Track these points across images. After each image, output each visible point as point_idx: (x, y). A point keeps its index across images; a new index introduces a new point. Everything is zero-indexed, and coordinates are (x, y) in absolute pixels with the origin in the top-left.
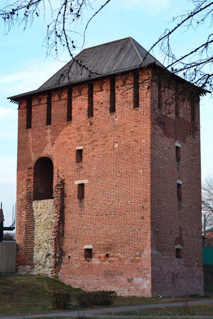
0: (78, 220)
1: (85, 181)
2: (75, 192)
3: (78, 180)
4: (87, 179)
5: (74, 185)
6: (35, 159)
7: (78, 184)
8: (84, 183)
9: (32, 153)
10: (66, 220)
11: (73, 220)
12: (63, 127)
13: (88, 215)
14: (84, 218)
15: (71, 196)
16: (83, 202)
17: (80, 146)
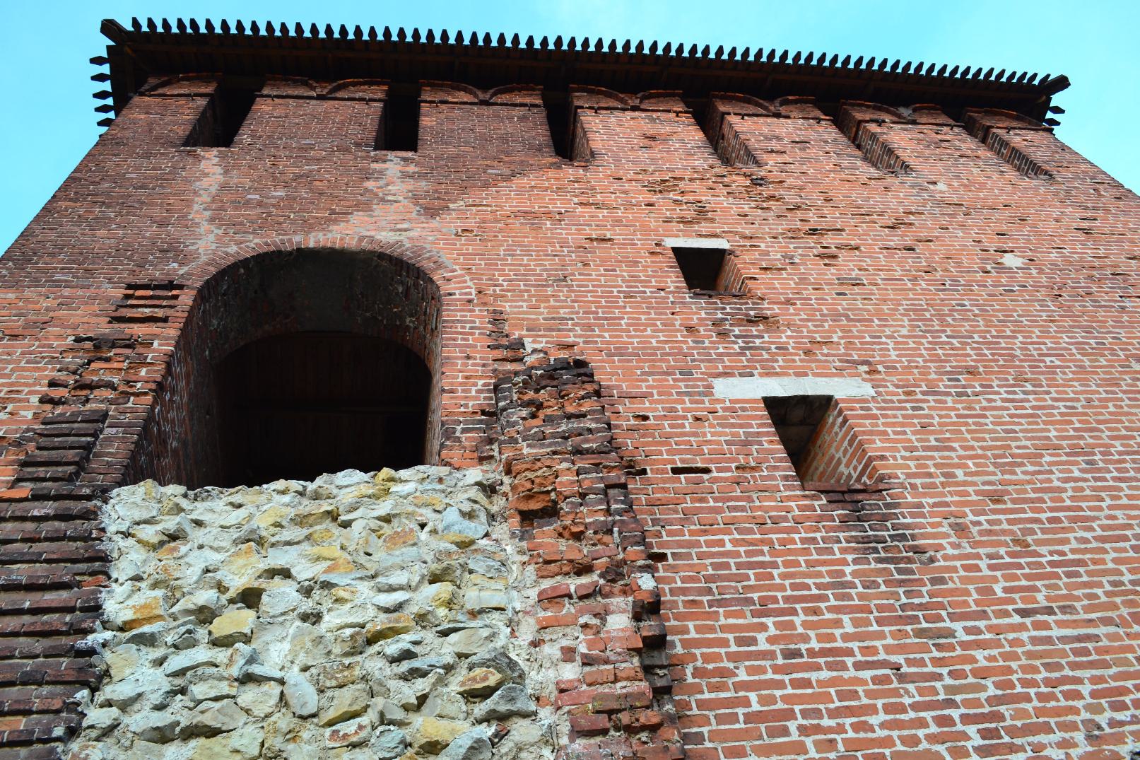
0: (903, 678)
1: (840, 388)
2: (746, 443)
3: (752, 375)
4: (859, 375)
5: (719, 401)
6: (233, 249)
7: (759, 397)
8: (826, 402)
9: (205, 226)
10: (698, 673)
11: (814, 676)
12: (519, 170)
13: (1017, 619)
14: (980, 655)
15: (707, 471)
16: (885, 518)
17: (700, 236)
